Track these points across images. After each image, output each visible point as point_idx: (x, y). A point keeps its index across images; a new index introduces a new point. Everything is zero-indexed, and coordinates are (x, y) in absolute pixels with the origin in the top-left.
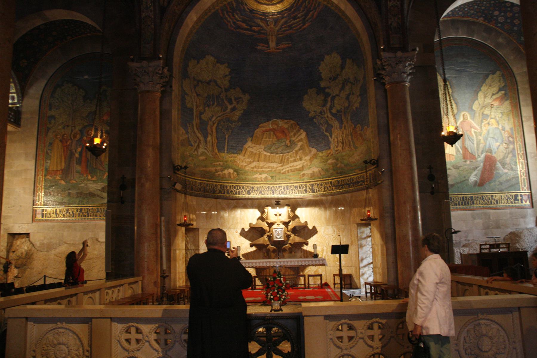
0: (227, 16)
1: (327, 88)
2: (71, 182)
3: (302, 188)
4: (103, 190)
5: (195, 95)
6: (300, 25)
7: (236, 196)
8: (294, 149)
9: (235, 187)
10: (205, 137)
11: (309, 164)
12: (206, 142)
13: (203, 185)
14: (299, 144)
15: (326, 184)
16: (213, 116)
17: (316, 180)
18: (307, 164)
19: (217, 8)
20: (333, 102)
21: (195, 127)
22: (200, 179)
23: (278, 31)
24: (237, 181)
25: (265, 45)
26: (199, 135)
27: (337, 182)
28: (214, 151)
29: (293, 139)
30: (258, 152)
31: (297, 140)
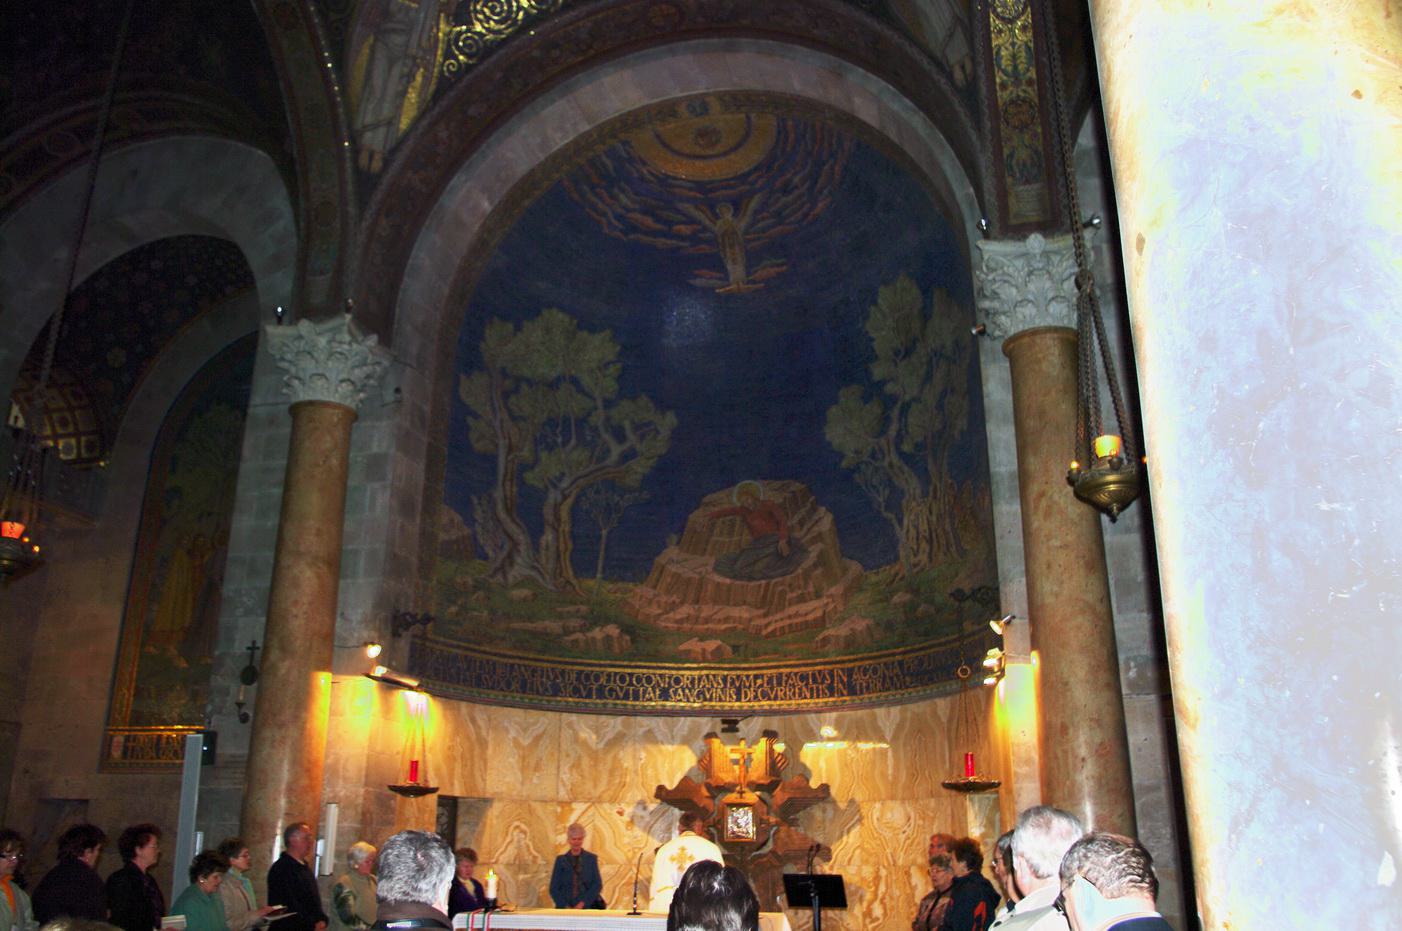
0: (594, 199)
1: (889, 381)
3: (819, 681)
5: (506, 417)
6: (805, 209)
7: (625, 705)
8: (799, 565)
9: (623, 679)
10: (536, 533)
11: (840, 608)
12: (535, 546)
13: (521, 673)
14: (814, 551)
15: (887, 669)
16: (563, 474)
17: (860, 656)
18: (835, 607)
19: (557, 176)
20: (903, 420)
21: (500, 507)
22: (510, 653)
23: (746, 232)
24: (632, 661)
25: (714, 274)
26: (513, 528)
27: (916, 662)
28: (561, 575)
29: (797, 534)
30: (697, 576)
31: (809, 536)
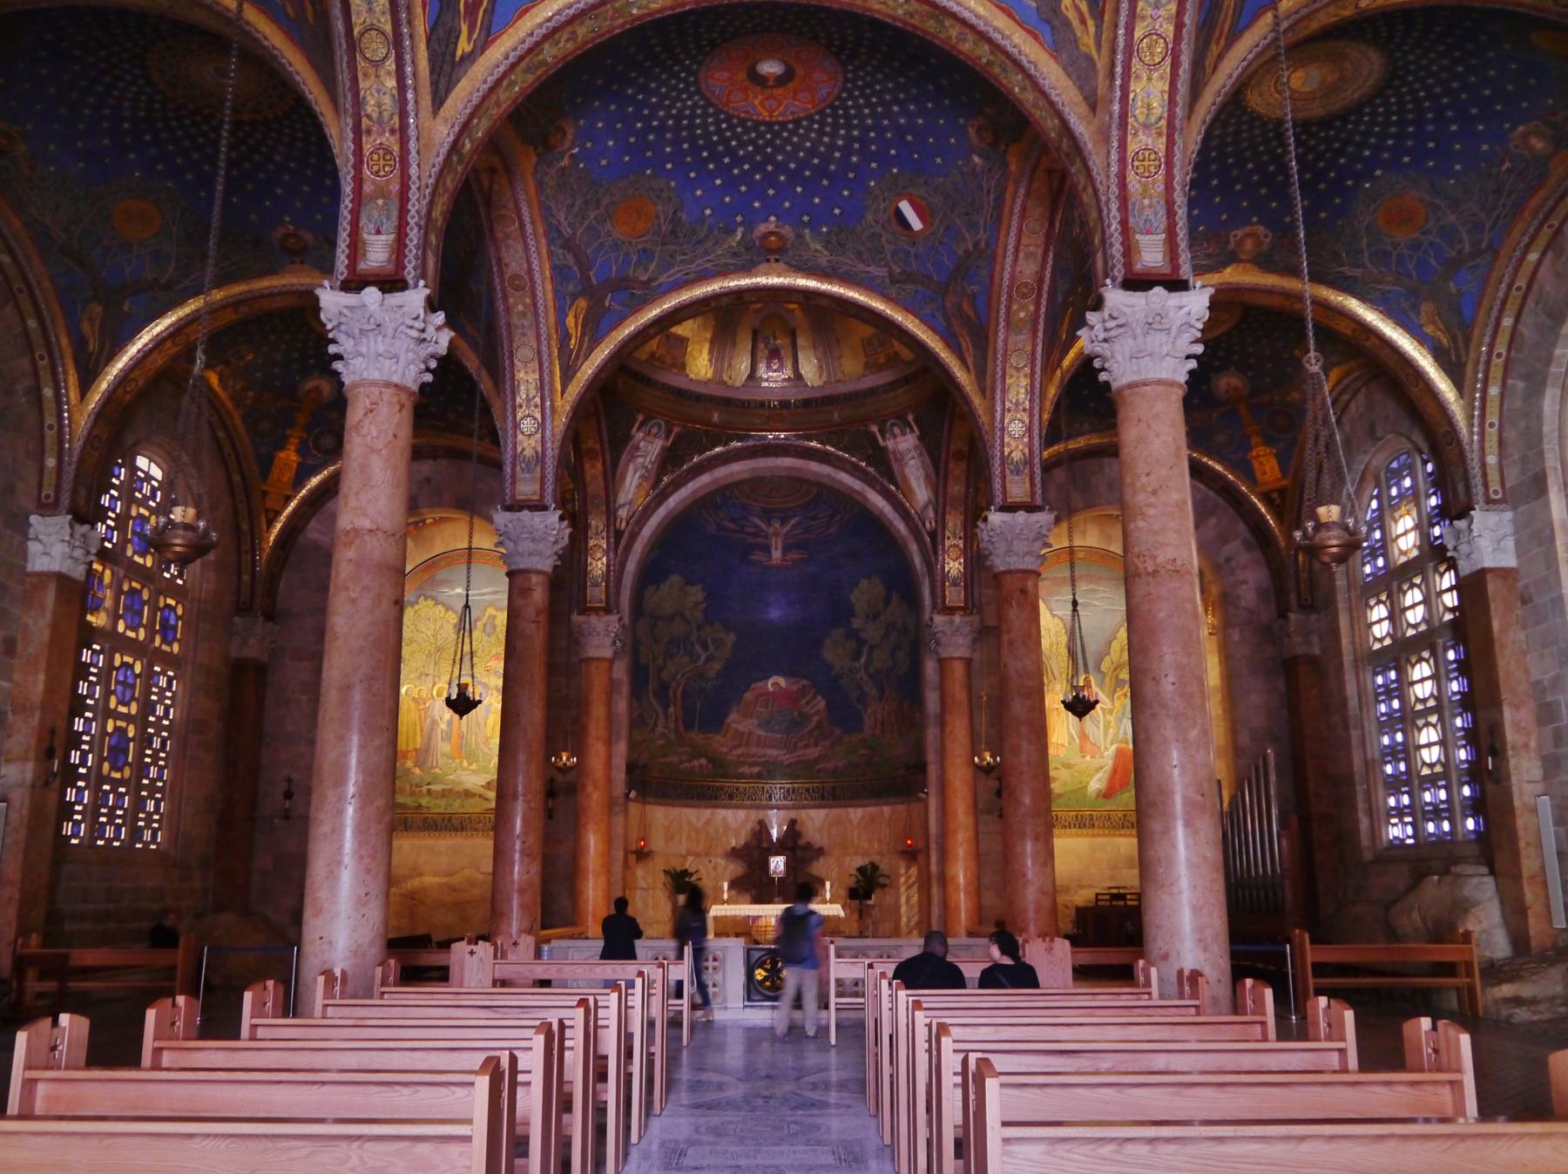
4: (488, 786)
10: (666, 707)
12: (666, 716)
23: (786, 534)
29: (805, 710)
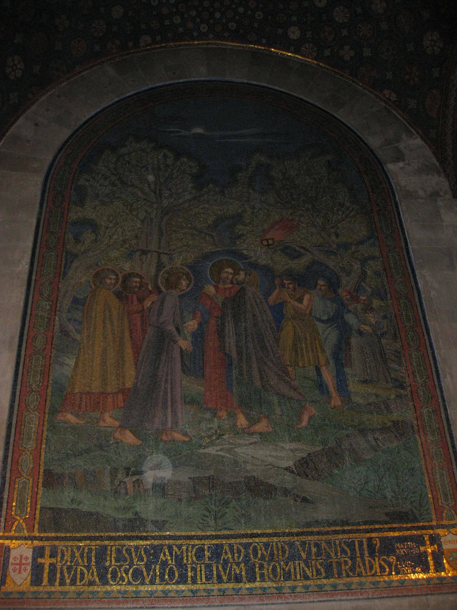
2: (164, 438)
